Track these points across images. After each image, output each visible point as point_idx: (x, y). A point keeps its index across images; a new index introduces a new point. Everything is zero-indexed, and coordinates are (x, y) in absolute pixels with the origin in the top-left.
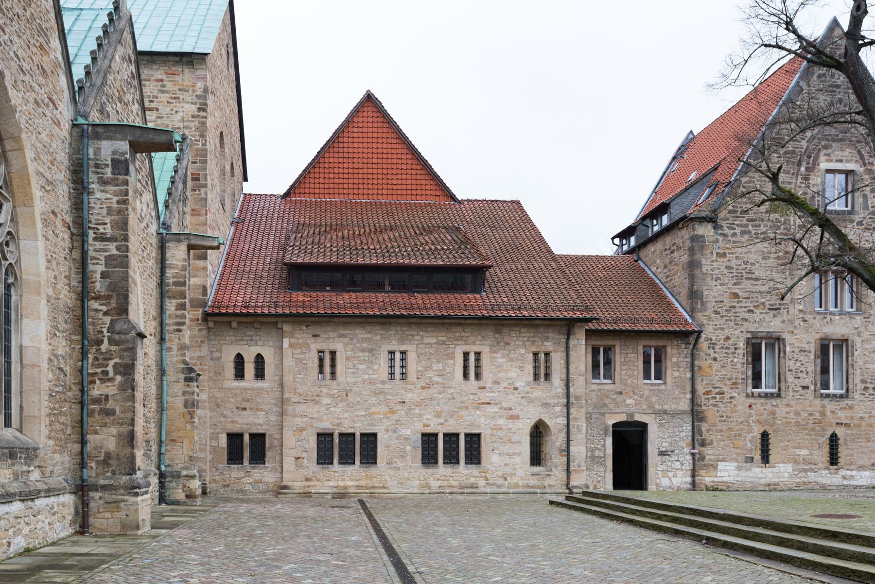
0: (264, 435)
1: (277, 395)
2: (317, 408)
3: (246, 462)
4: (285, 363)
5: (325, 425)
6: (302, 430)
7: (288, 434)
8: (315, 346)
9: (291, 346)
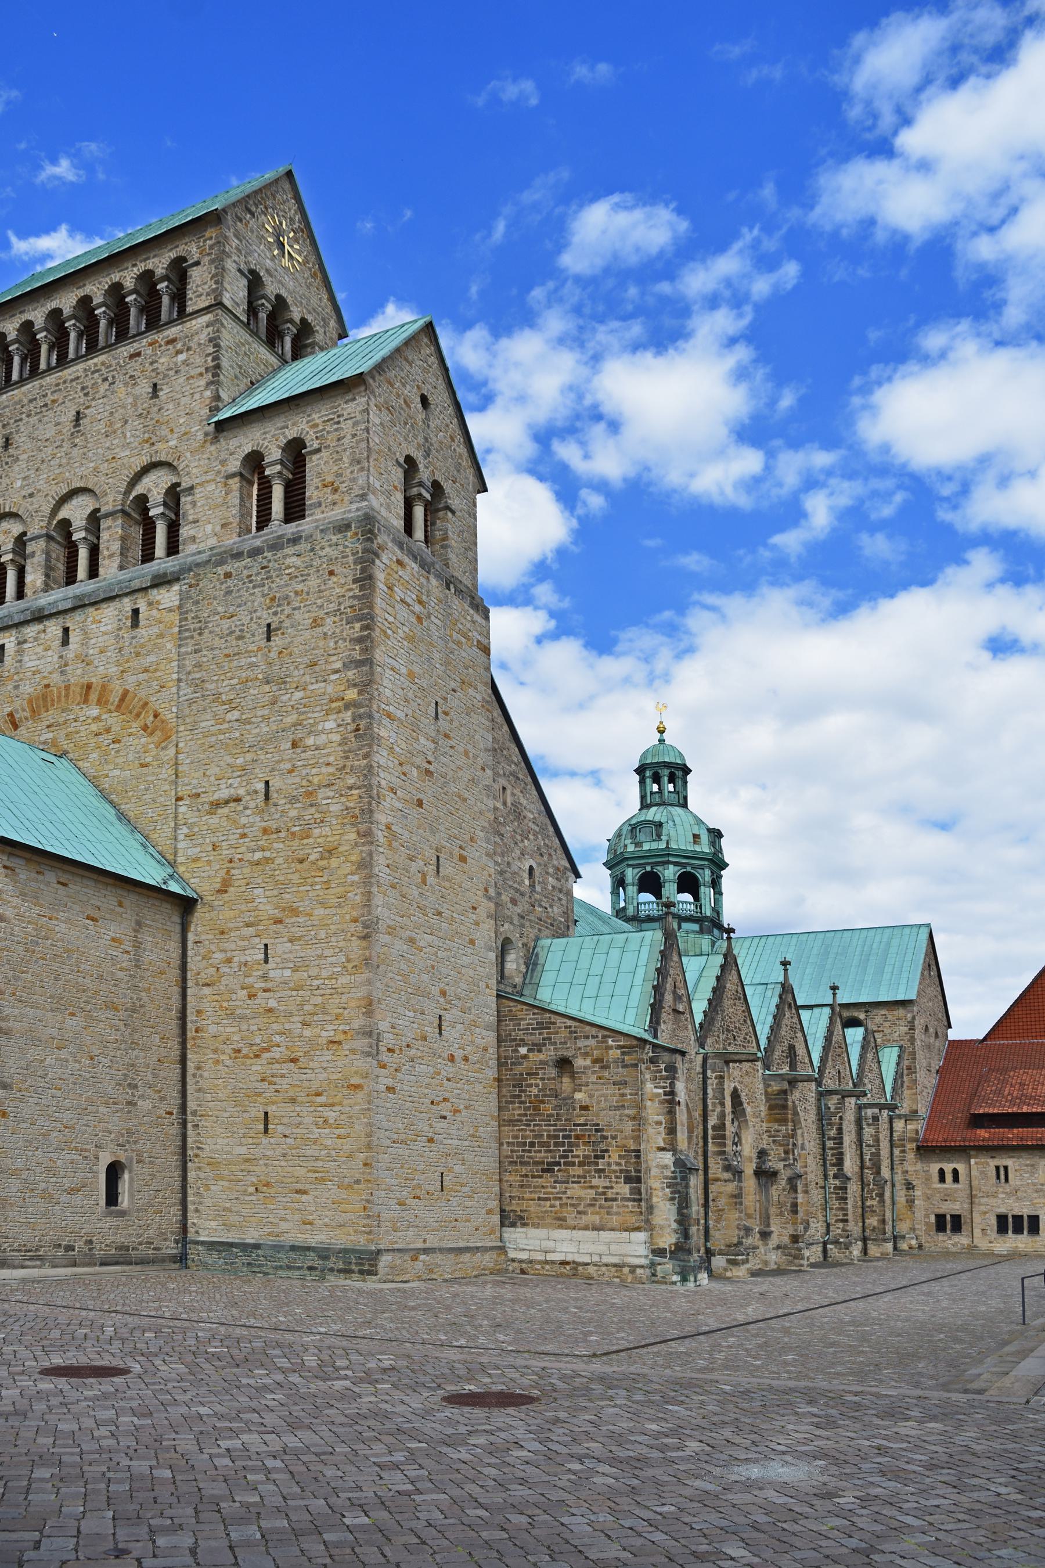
0: (960, 1216)
1: (968, 1192)
2: (995, 1200)
3: (948, 1232)
4: (973, 1173)
5: (1002, 1210)
6: (986, 1213)
7: (975, 1215)
8: (993, 1163)
9: (976, 1163)
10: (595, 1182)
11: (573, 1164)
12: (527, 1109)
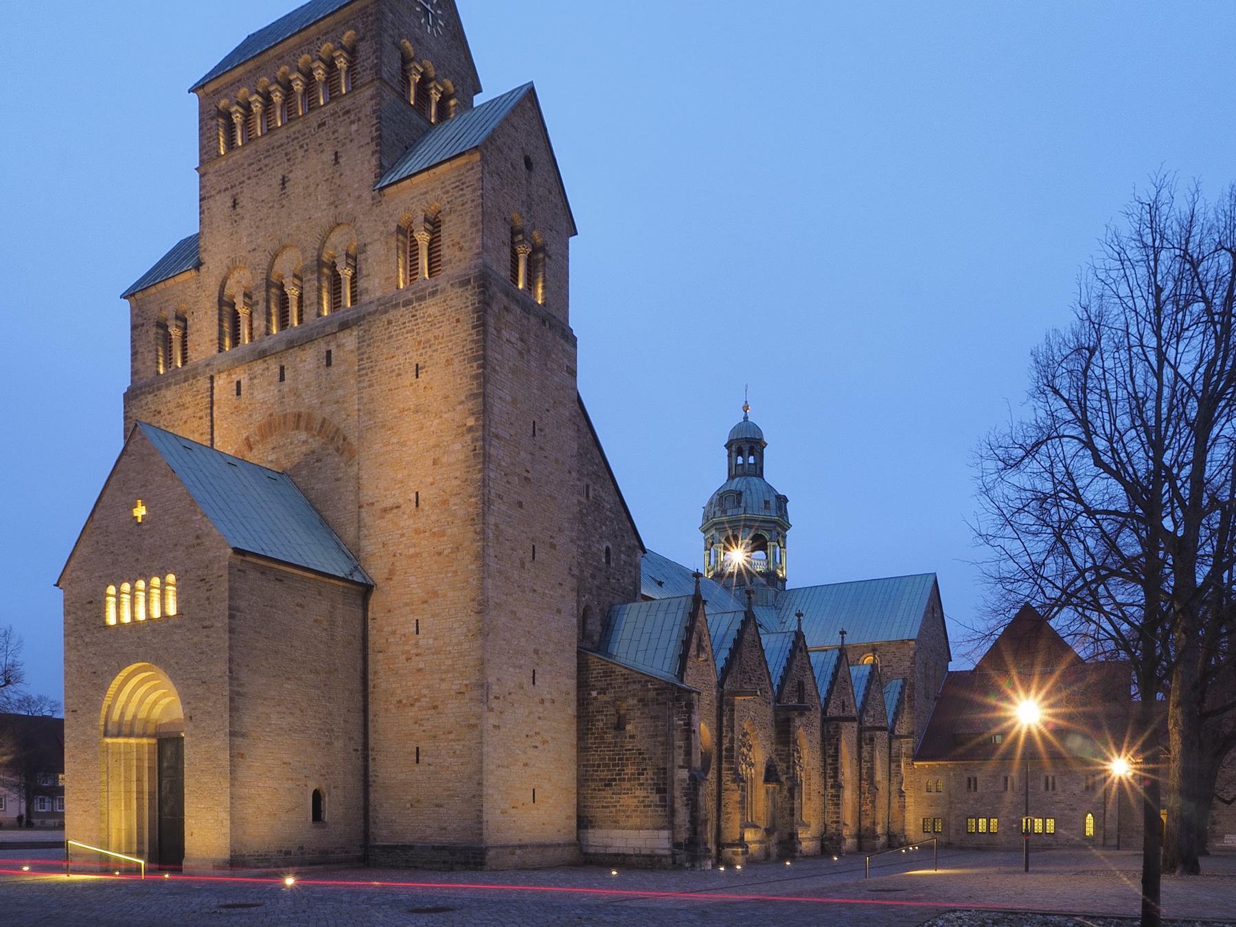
10: (638, 793)
11: (624, 780)
12: (596, 738)
